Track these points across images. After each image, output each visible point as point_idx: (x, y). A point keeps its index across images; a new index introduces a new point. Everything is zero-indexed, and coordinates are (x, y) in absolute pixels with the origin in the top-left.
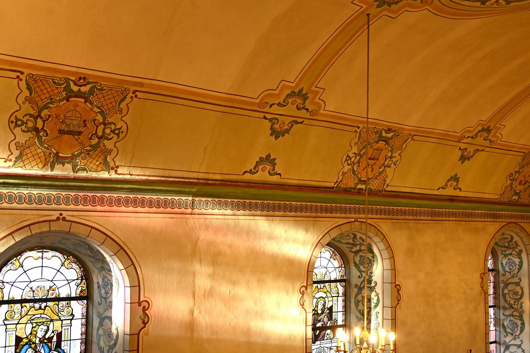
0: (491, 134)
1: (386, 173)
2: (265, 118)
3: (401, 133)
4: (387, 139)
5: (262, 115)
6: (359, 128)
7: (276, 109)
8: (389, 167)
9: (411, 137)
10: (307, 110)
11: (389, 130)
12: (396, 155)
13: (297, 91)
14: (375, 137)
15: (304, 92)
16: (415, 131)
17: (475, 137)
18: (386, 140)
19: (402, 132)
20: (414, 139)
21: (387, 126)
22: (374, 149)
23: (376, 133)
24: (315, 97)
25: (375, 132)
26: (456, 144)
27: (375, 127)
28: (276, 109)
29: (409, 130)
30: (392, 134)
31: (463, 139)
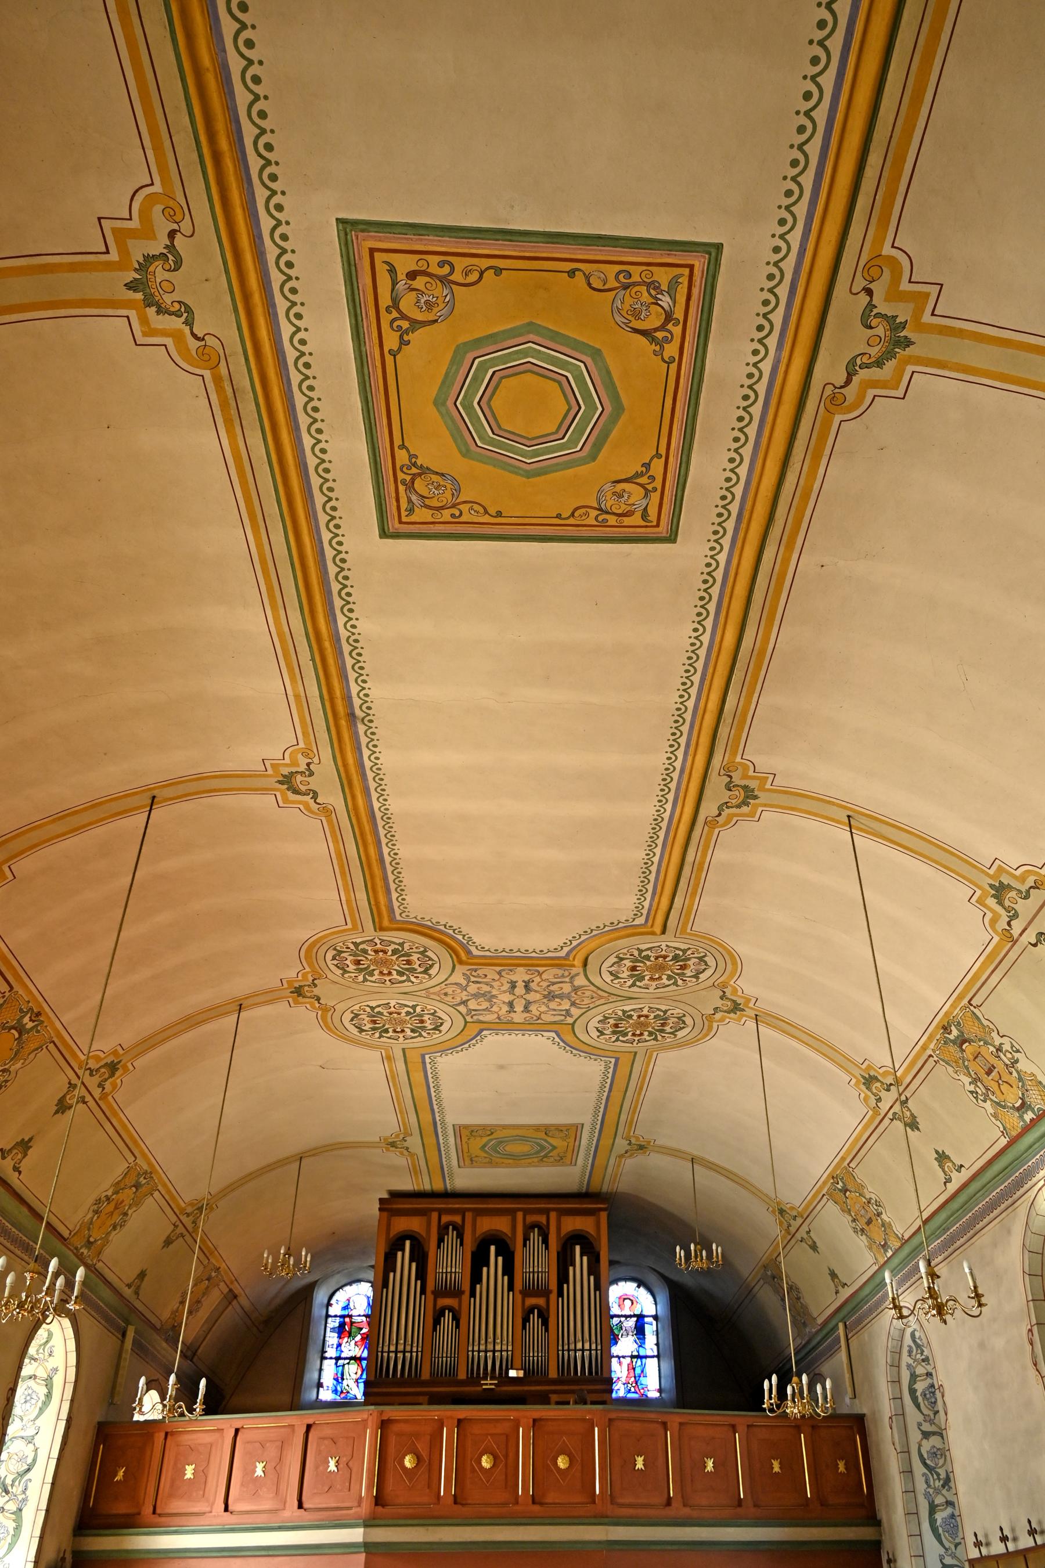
0: (1014, 884)
1: (1025, 1072)
2: (892, 1120)
3: (955, 1018)
4: (960, 1038)
5: (886, 1121)
6: (930, 1056)
7: (884, 1106)
8: (1017, 1061)
9: (972, 1008)
10: (891, 1084)
11: (946, 1029)
12: (998, 1041)
13: (863, 1081)
14: (953, 1049)
15: (867, 1076)
16: (960, 998)
17: (1013, 912)
18: (962, 1041)
19: (954, 1017)
20: (979, 1005)
21: (937, 1027)
22: (974, 1060)
23: (945, 1043)
24: (875, 1070)
25: (944, 1044)
26: (1017, 949)
27: (937, 1040)
28: (884, 1106)
29: (953, 1006)
30: (953, 1028)
31: (1012, 936)
